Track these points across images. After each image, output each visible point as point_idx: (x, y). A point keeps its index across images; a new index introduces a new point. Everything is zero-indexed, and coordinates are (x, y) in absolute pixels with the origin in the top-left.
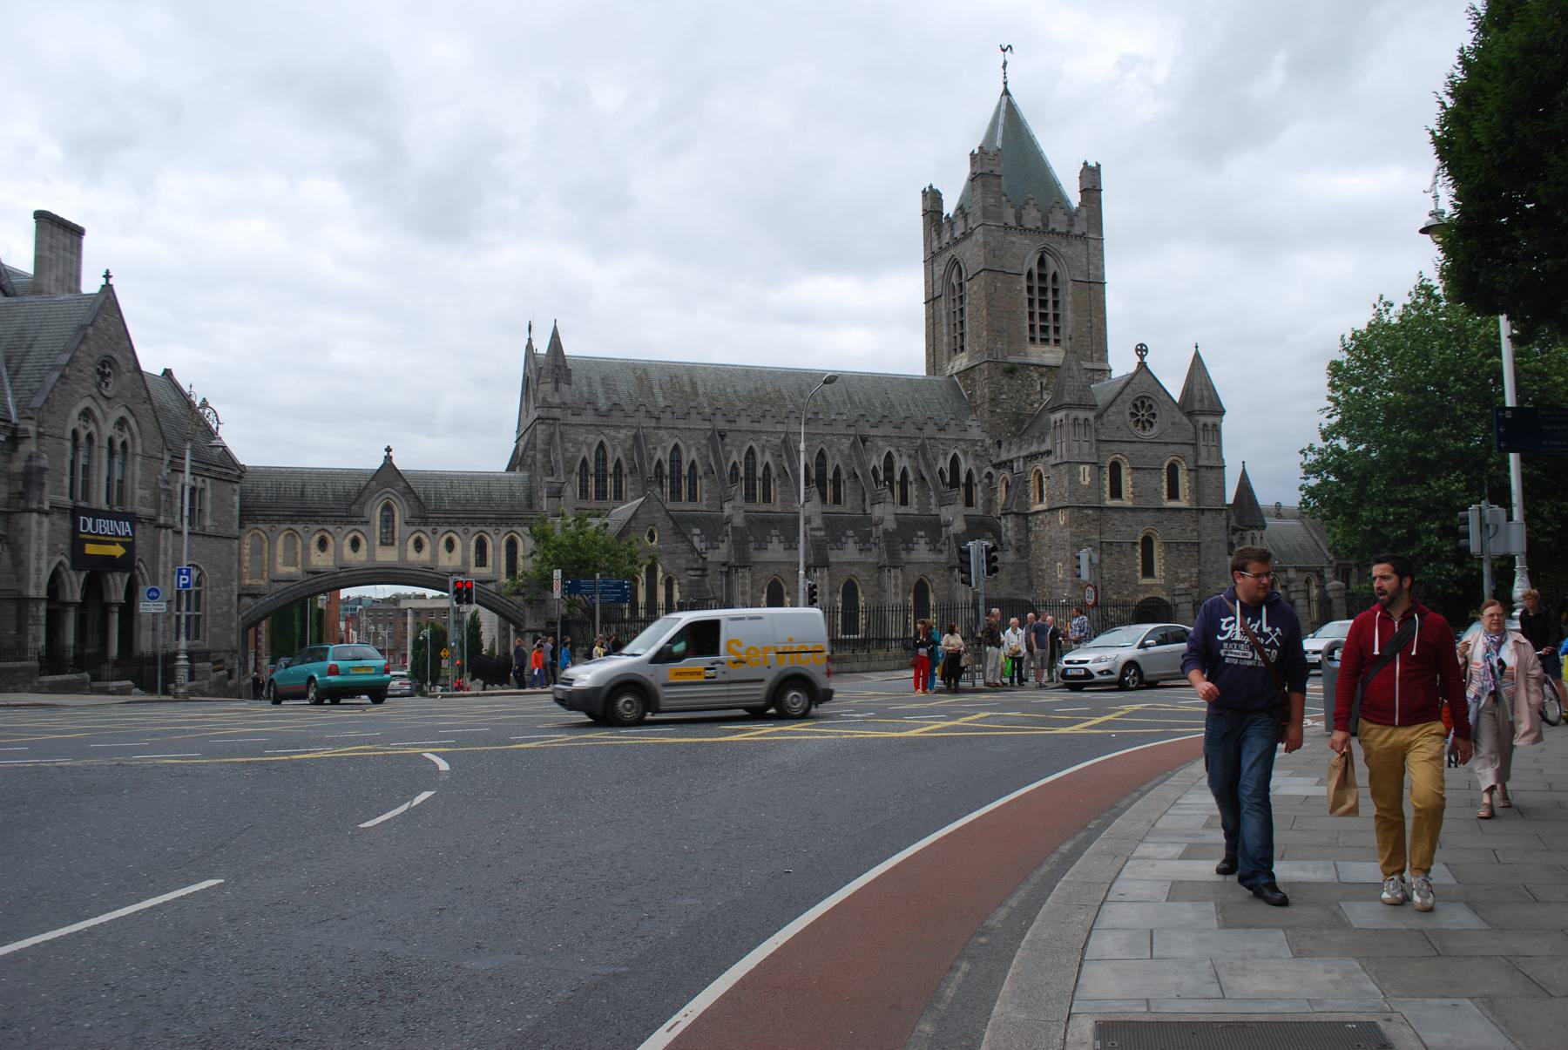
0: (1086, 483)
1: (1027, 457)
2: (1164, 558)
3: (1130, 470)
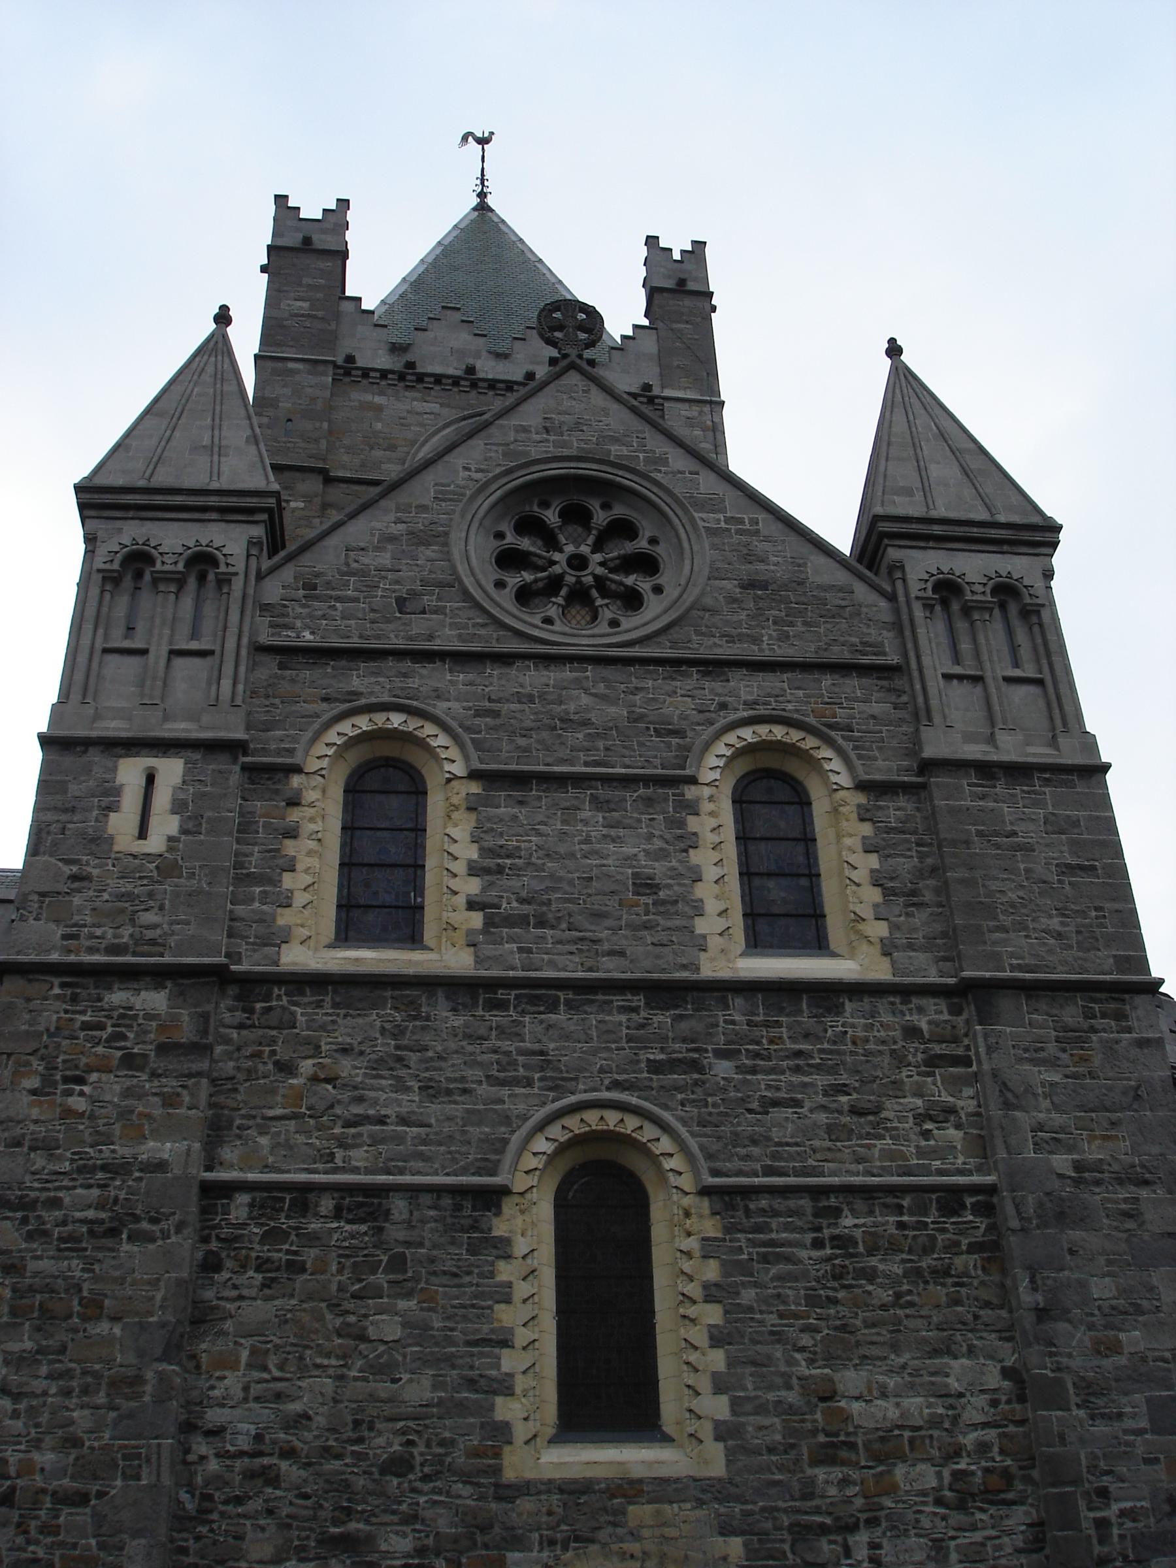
0: (155, 844)
2: (712, 1293)
3: (475, 788)
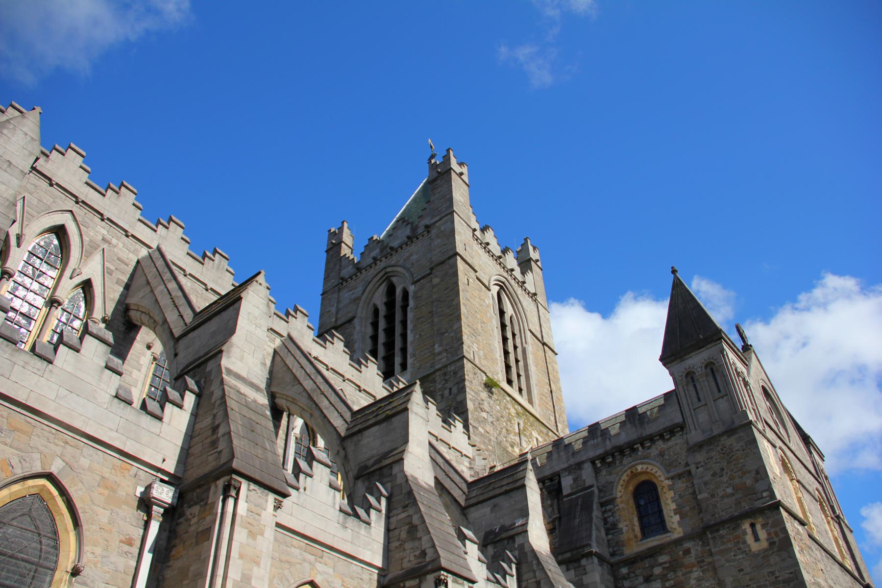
1: (602, 458)
